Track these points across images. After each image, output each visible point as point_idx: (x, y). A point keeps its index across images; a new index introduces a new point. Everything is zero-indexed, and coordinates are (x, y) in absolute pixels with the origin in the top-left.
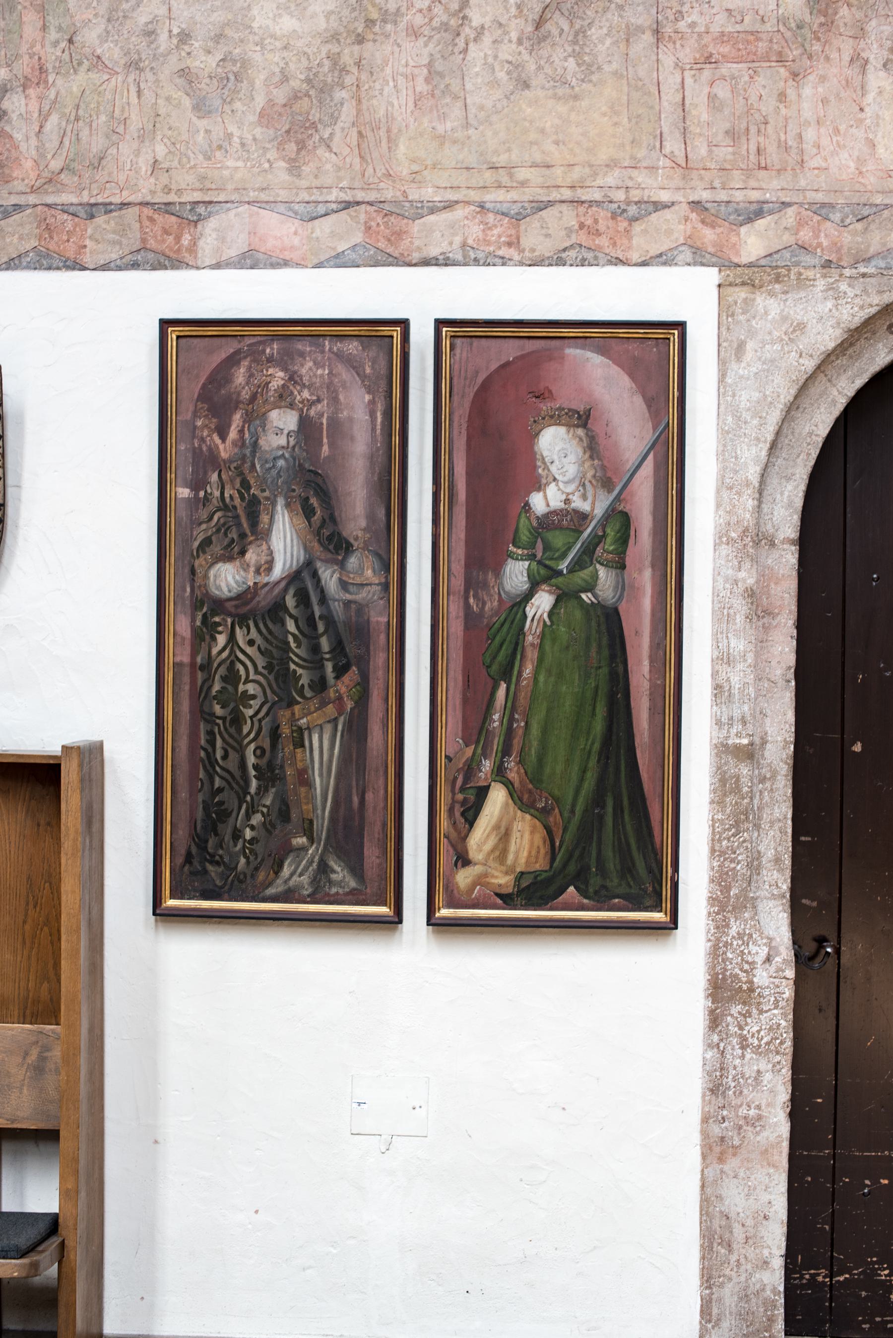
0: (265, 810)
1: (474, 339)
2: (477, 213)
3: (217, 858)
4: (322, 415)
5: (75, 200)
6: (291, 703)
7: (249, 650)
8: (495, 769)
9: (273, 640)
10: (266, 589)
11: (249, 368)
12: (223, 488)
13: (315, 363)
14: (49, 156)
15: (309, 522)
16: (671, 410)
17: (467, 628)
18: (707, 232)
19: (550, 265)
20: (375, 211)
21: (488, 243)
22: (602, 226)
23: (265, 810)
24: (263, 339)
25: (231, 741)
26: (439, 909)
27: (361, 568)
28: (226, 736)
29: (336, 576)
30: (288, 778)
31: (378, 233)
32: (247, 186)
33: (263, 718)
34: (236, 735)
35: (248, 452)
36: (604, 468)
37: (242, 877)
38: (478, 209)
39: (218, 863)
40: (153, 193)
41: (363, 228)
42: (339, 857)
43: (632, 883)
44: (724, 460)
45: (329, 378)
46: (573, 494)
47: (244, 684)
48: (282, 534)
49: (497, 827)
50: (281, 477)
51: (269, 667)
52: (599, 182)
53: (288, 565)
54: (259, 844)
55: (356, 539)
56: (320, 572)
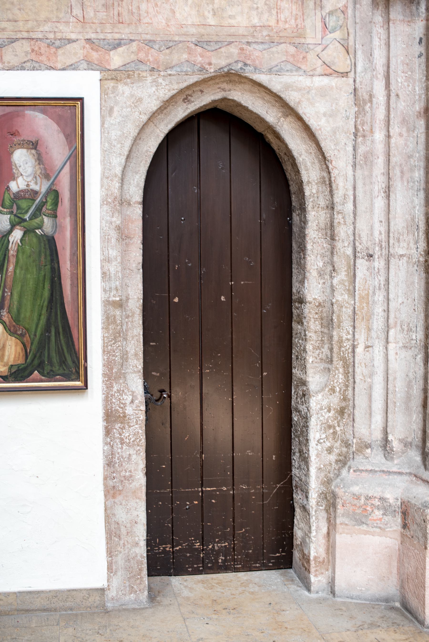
16: (77, 140)
22: (42, 51)
36: (45, 169)
43: (65, 368)
46: (31, 182)
52: (41, 29)
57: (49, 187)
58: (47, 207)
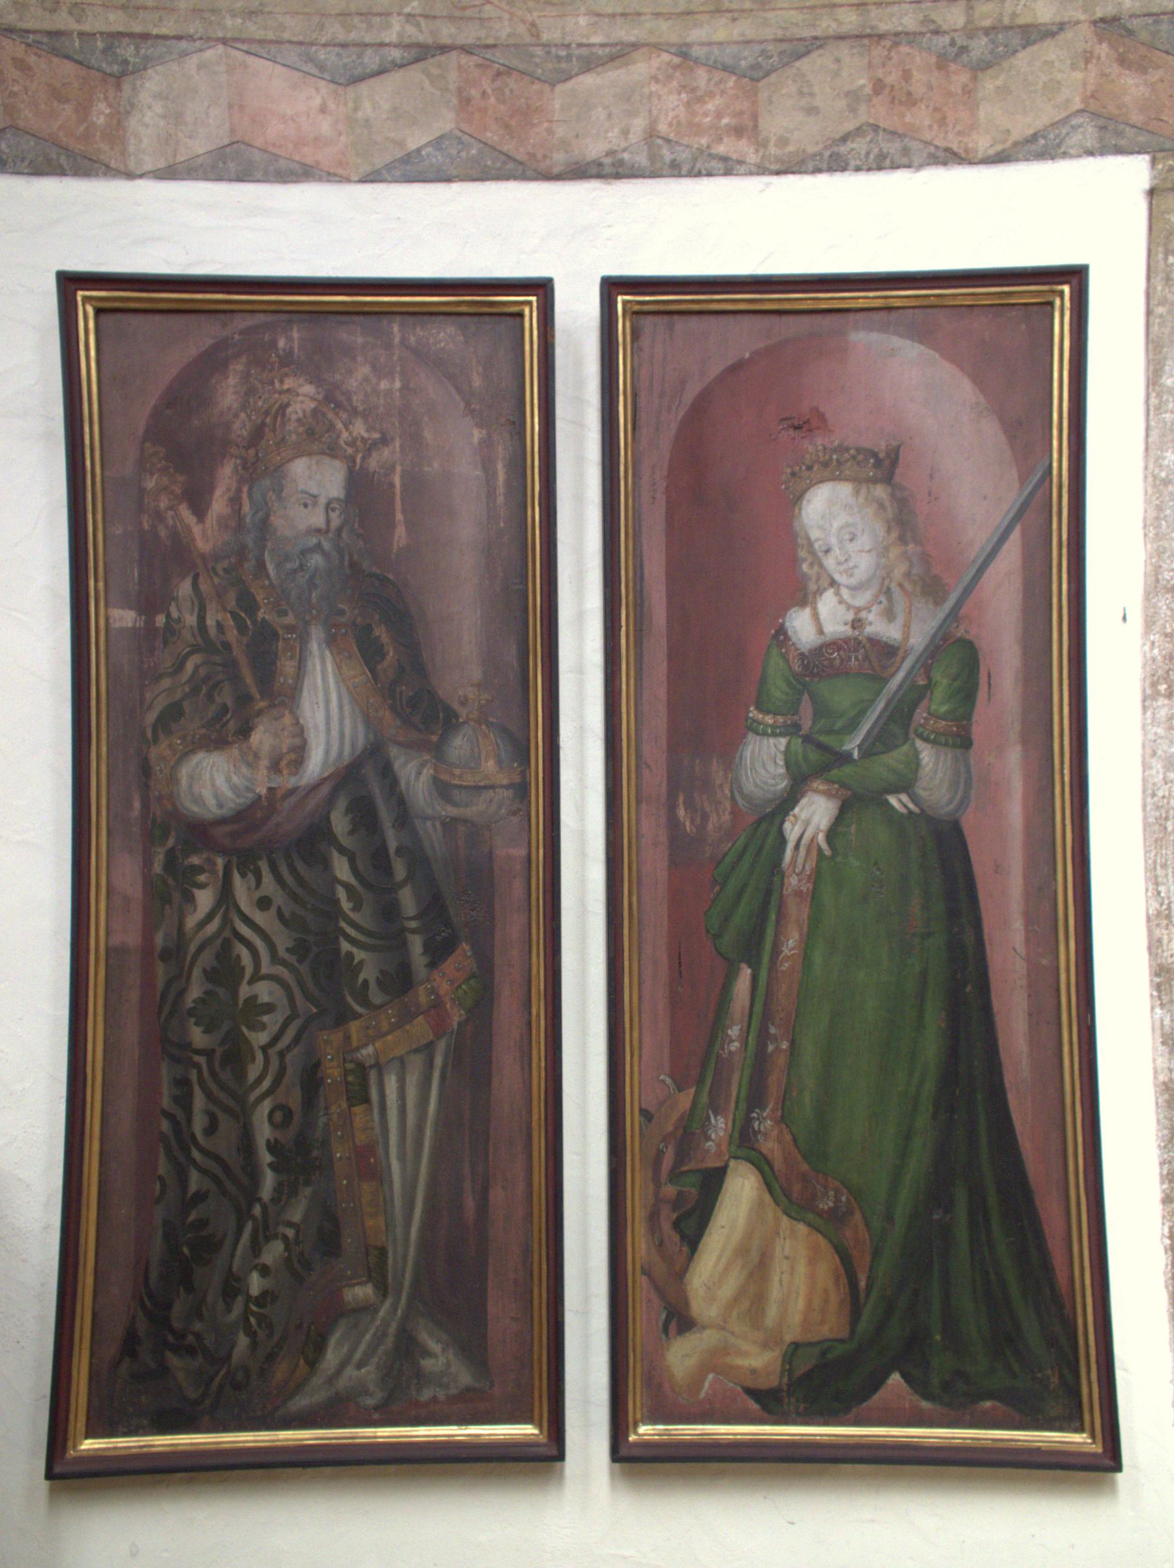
0: (290, 1233)
1: (675, 317)
2: (677, 67)
3: (190, 1339)
4: (393, 468)
6: (343, 1017)
7: (259, 917)
8: (736, 1135)
10: (293, 800)
11: (246, 377)
12: (202, 611)
13: (374, 367)
15: (372, 671)
16: (1055, 443)
17: (673, 863)
18: (1130, 82)
19: (817, 170)
20: (478, 66)
21: (697, 129)
22: (918, 89)
25: (222, 1096)
26: (636, 1425)
29: (427, 772)
33: (289, 1048)
35: (249, 541)
36: (925, 558)
37: (240, 1376)
38: (677, 60)
39: (191, 1351)
41: (455, 101)
43: (1016, 1367)
44: (1158, 537)
46: (868, 609)
47: (251, 982)
48: (321, 694)
49: (742, 1251)
50: (315, 586)
51: (300, 949)
53: (334, 754)
55: (464, 702)
56: (397, 765)
57: (940, 627)
58: (933, 707)
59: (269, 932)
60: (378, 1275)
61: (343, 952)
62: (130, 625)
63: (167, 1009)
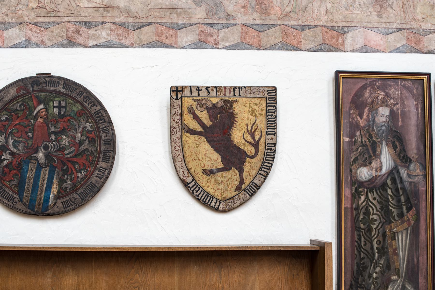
0: (381, 266)
3: (362, 286)
4: (399, 109)
5: (296, 24)
6: (390, 222)
7: (374, 202)
9: (383, 198)
10: (380, 177)
11: (370, 91)
12: (362, 138)
13: (395, 89)
14: (285, 6)
15: (395, 151)
20: (410, 32)
23: (381, 266)
24: (375, 79)
25: (367, 238)
27: (415, 169)
28: (365, 236)
29: (406, 172)
30: (390, 252)
31: (412, 41)
32: (362, 21)
33: (380, 229)
34: (369, 236)
35: (371, 123)
40: (327, 22)
41: (406, 38)
42: (410, 284)
45: (401, 95)
47: (372, 215)
50: (384, 133)
51: (382, 208)
53: (388, 168)
54: (379, 279)
55: (413, 157)
56: (400, 170)
59: (375, 204)
60: (398, 274)
61: (390, 209)
62: (348, 141)
63: (356, 220)
